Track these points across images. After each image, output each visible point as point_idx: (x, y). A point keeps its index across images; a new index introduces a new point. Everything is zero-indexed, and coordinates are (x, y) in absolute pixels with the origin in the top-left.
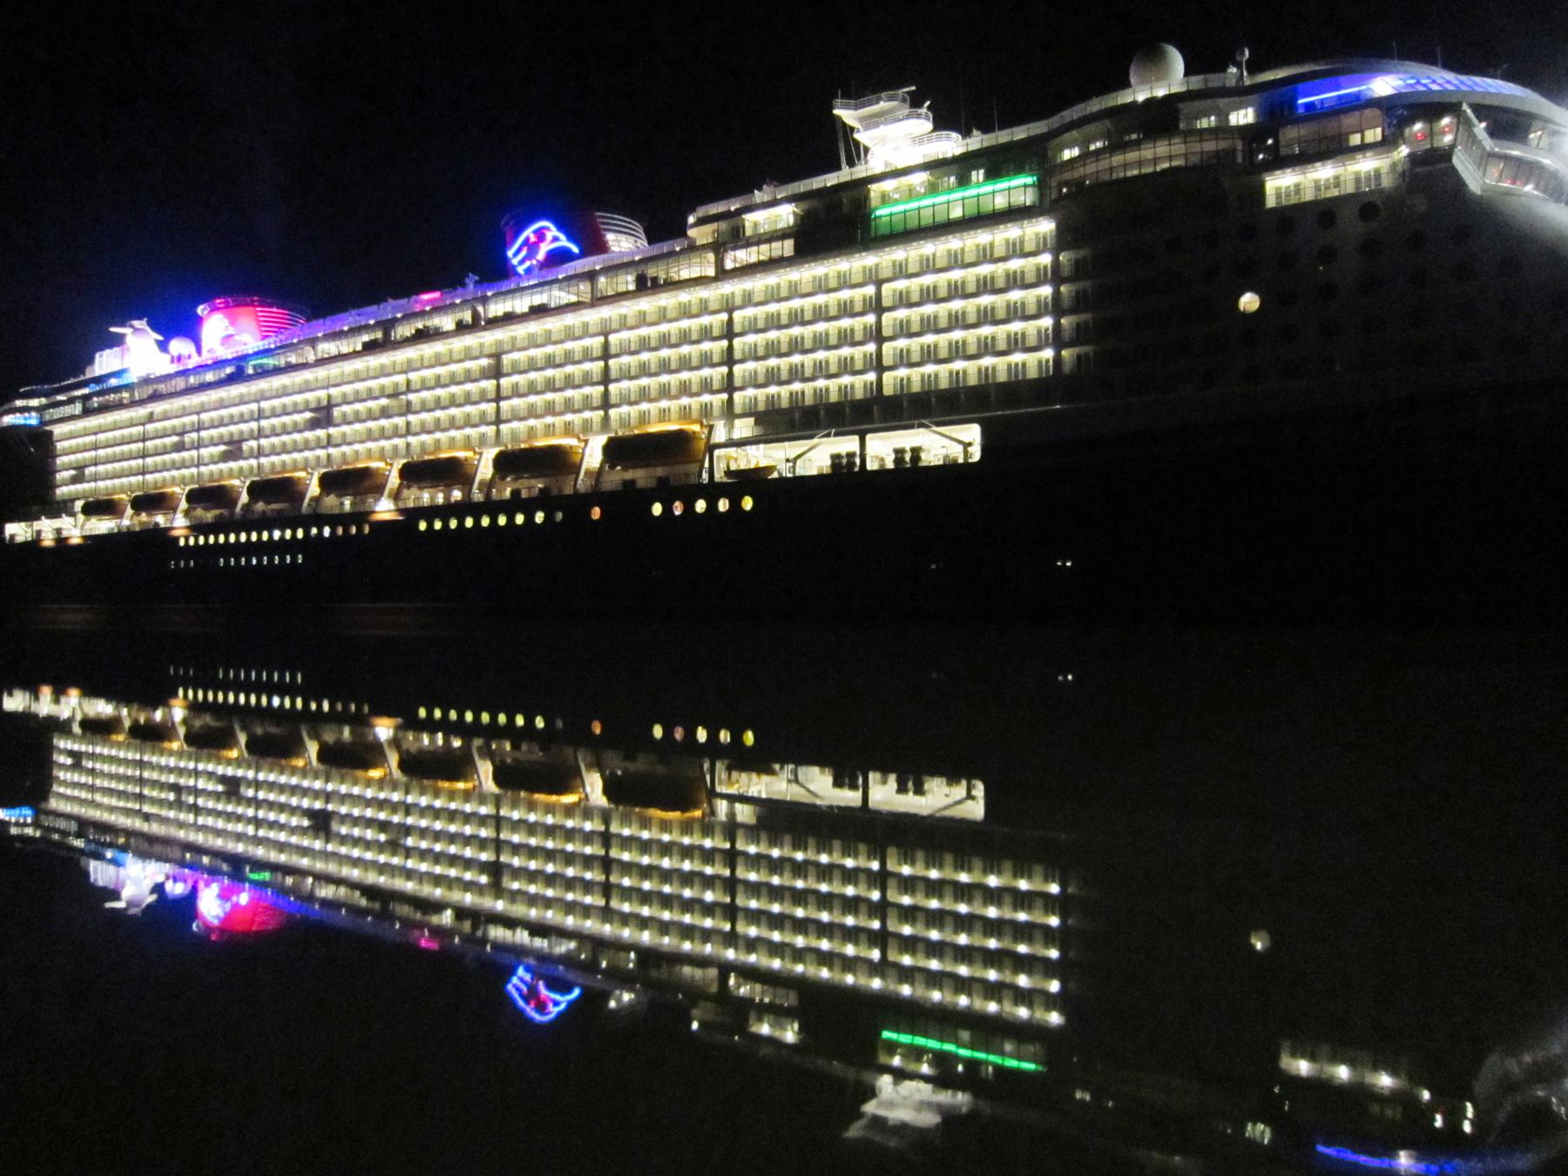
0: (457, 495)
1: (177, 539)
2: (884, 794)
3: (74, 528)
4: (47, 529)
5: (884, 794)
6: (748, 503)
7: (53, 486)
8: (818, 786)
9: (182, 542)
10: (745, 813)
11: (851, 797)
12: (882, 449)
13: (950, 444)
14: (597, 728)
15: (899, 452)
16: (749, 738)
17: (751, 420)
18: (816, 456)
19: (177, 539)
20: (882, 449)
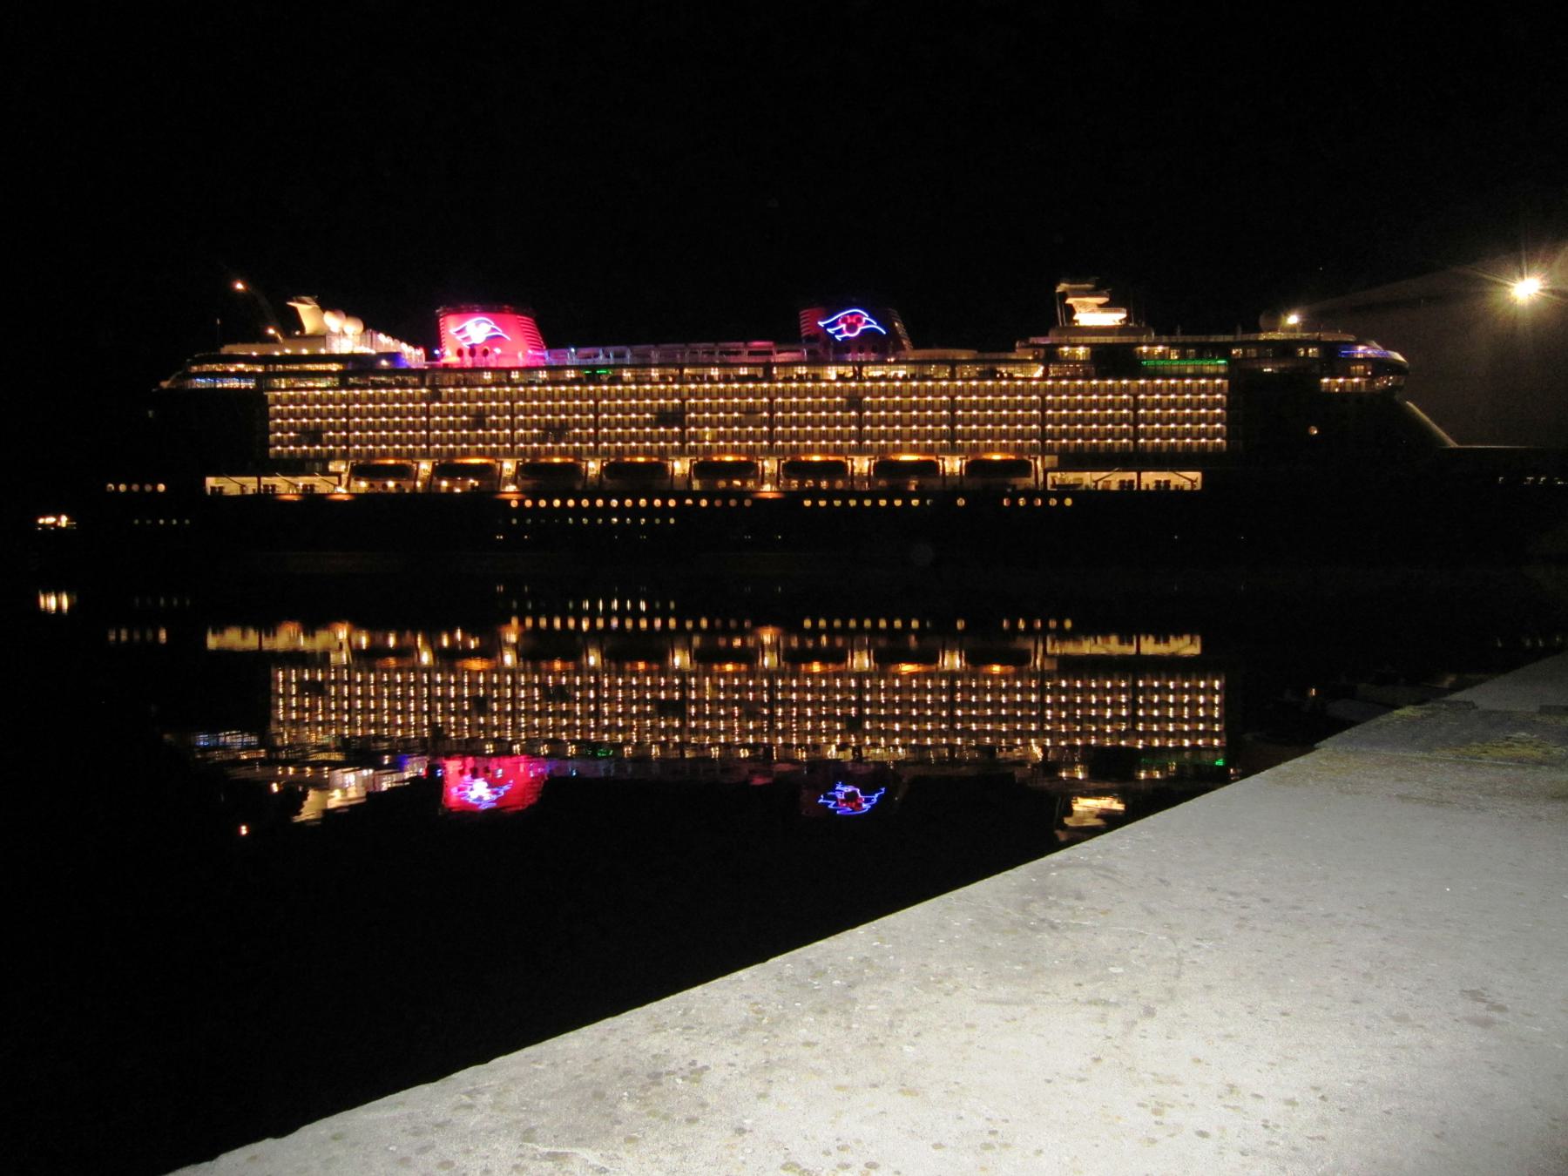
0: (839, 484)
1: (509, 501)
2: (1149, 647)
3: (339, 485)
4: (286, 487)
5: (1149, 647)
6: (1068, 502)
7: (267, 445)
8: (1112, 646)
9: (514, 504)
10: (1051, 666)
11: (1132, 650)
12: (1150, 479)
13: (1187, 479)
14: (960, 625)
15: (1158, 482)
16: (1068, 624)
17: (1055, 458)
18: (1114, 479)
19: (509, 501)
20: (1150, 479)
